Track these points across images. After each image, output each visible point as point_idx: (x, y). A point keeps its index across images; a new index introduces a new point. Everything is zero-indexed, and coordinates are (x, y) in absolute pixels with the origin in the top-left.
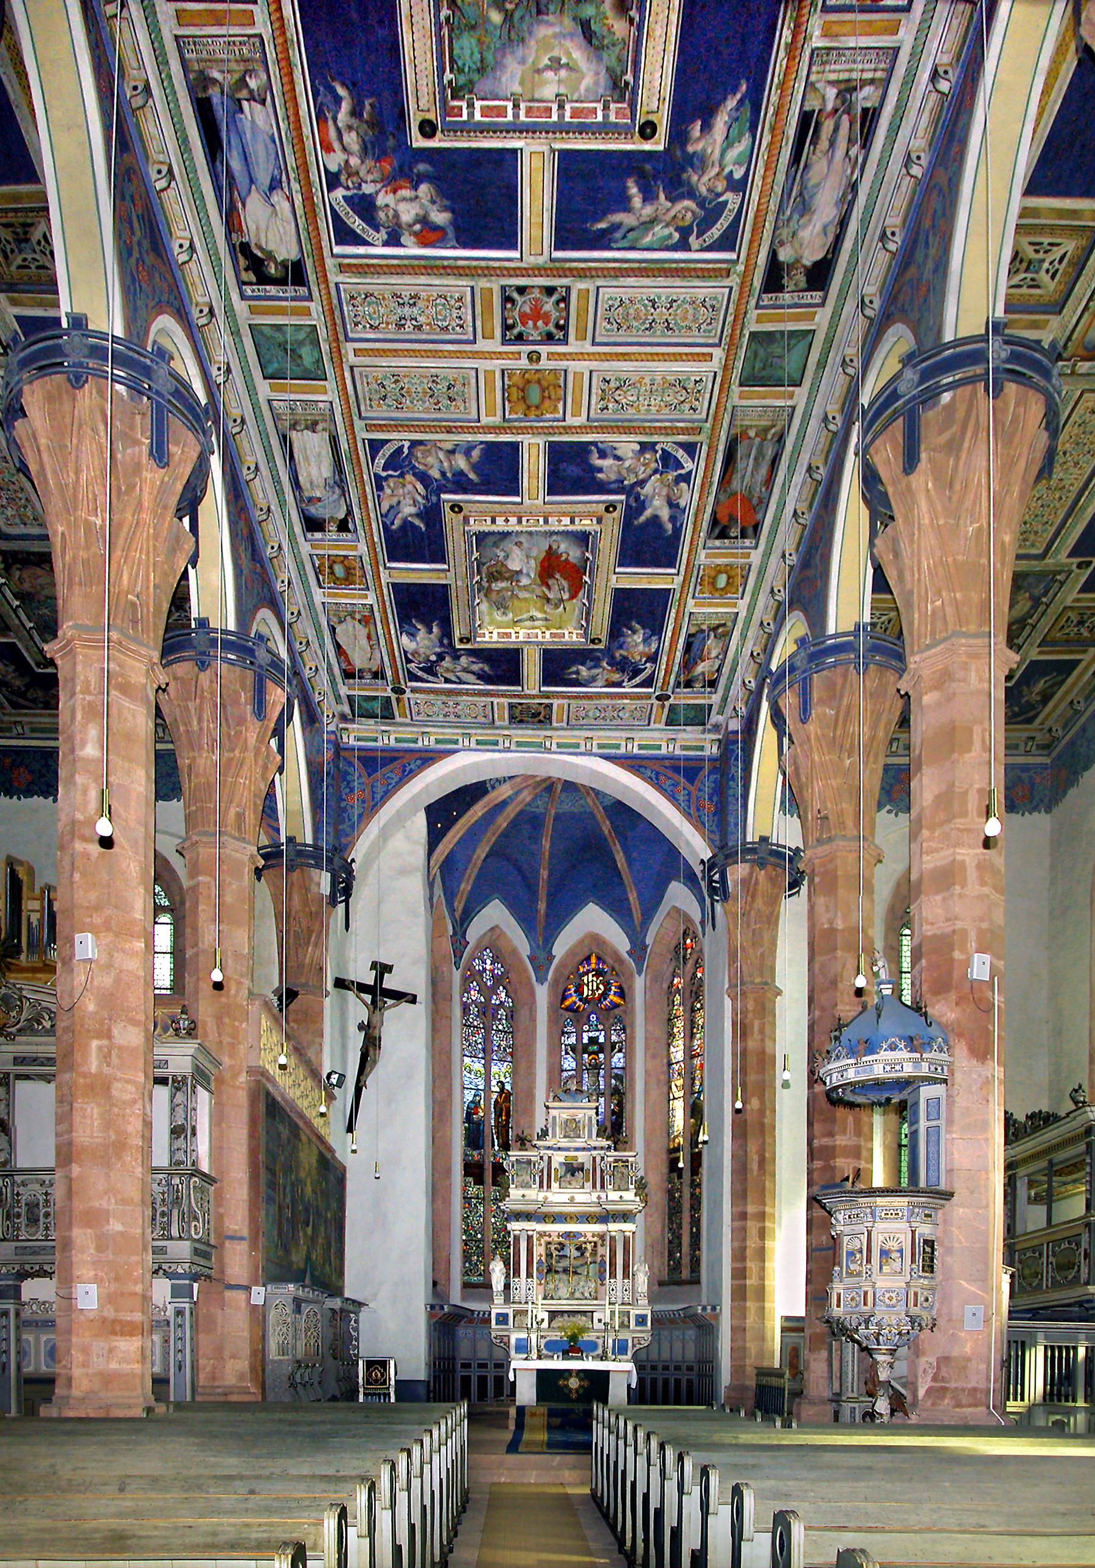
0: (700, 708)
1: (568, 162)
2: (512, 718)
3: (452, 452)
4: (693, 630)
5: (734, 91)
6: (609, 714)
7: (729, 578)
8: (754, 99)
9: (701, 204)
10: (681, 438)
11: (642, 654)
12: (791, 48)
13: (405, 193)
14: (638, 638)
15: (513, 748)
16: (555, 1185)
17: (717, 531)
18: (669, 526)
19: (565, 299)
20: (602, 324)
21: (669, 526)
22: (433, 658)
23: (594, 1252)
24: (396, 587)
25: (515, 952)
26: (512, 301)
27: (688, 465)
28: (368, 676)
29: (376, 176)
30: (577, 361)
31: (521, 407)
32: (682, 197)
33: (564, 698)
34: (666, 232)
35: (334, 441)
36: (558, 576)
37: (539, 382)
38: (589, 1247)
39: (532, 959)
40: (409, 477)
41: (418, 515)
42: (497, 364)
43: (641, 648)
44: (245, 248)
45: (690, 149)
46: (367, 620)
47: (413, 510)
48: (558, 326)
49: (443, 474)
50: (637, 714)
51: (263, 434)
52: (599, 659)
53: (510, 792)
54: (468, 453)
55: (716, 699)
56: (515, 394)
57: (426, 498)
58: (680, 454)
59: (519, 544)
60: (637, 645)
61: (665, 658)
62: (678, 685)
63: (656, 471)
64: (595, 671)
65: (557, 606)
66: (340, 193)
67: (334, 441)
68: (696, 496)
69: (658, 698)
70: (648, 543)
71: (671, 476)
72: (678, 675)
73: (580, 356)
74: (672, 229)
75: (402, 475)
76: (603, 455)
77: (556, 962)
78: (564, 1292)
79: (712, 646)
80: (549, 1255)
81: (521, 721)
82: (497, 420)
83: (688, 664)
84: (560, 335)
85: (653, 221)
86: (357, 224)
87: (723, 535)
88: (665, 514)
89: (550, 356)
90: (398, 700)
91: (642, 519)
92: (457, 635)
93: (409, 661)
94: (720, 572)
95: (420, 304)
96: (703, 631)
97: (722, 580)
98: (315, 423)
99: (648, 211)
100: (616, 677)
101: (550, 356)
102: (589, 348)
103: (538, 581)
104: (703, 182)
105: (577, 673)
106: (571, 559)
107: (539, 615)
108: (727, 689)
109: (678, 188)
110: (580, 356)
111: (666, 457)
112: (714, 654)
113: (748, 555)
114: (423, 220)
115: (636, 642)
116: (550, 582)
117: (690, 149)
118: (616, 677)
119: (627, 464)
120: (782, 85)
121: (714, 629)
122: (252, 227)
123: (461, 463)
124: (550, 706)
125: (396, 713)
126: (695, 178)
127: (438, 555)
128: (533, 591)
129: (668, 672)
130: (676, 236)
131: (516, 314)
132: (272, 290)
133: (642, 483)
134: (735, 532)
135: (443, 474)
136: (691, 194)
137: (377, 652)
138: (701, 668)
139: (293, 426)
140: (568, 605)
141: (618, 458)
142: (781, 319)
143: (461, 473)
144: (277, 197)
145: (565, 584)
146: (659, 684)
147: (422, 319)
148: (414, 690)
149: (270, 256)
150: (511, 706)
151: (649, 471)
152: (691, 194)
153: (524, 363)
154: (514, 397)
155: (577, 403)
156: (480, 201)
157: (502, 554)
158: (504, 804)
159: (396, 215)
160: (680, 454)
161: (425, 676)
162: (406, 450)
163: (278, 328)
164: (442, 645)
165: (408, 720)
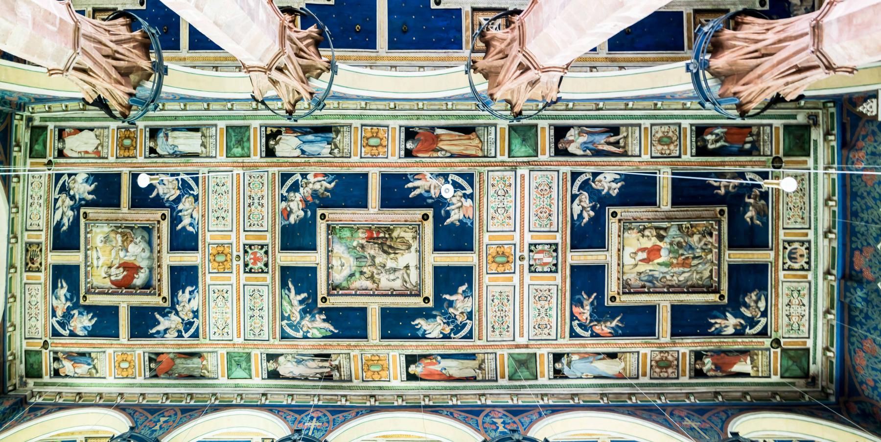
1: (313, 270)
3: (192, 217)
4: (93, 355)
5: (335, 328)
6: (33, 311)
8: (334, 336)
9: (299, 323)
10: (201, 331)
11: (75, 328)
12: (349, 345)
13: (301, 206)
17: (153, 356)
18: (154, 331)
19: (263, 272)
20: (252, 288)
21: (154, 331)
26: (262, 249)
27: (186, 335)
29: (306, 194)
30: (236, 277)
31: (215, 252)
32: (301, 315)
33: (46, 280)
34: (288, 311)
35: (196, 155)
36: (125, 273)
37: (226, 260)
40: (178, 192)
41: (158, 194)
42: (233, 240)
44: (279, 133)
45: (317, 316)
47: (161, 193)
48: (251, 269)
49: (181, 211)
50: (33, 330)
51: (199, 118)
52: (71, 300)
54: (191, 224)
56: (221, 249)
57: (168, 200)
58: (192, 331)
60: (81, 323)
61: (74, 341)
62: (56, 353)
63: (183, 320)
64: (63, 299)
65: (106, 273)
66: (300, 178)
67: (196, 155)
68: (172, 342)
70: (143, 322)
71: (181, 328)
73: (238, 280)
74: (289, 312)
75: (179, 189)
76: (191, 293)
79: (83, 369)
82: (208, 240)
83: (70, 356)
84: (247, 270)
85: (292, 305)
86: (289, 182)
87: (151, 360)
88: (160, 328)
89: (238, 266)
91: (158, 316)
94: (130, 363)
95: (259, 208)
96: (93, 361)
97: (124, 365)
98: (205, 147)
99: (296, 303)
101: (238, 266)
102: (242, 282)
103: (122, 262)
104: (306, 322)
107: (100, 264)
109: (304, 312)
110: (238, 280)
111: (191, 324)
112: (77, 370)
114: (291, 212)
115: (82, 322)
116: (121, 269)
117: (317, 316)
119: (187, 305)
120: (339, 345)
121: (94, 367)
122: (288, 138)
123: (186, 221)
124: (39, 271)
126: (307, 319)
128: (115, 259)
129: (63, 345)
130: (286, 315)
131: (256, 250)
132: (264, 140)
133: (177, 313)
134: (153, 365)
135: (181, 211)
136: (302, 318)
139: (203, 135)
140: (108, 280)
141: (190, 300)
142: (256, 363)
143: (181, 221)
144: (298, 152)
145: (120, 277)
146: (55, 341)
147: (253, 207)
149: (277, 143)
151: (183, 317)
152: (302, 318)
153: (235, 254)
154: (219, 249)
155: (216, 279)
156: (297, 236)
159: (292, 201)
160: (192, 331)
162: (192, 192)
163: (249, 140)
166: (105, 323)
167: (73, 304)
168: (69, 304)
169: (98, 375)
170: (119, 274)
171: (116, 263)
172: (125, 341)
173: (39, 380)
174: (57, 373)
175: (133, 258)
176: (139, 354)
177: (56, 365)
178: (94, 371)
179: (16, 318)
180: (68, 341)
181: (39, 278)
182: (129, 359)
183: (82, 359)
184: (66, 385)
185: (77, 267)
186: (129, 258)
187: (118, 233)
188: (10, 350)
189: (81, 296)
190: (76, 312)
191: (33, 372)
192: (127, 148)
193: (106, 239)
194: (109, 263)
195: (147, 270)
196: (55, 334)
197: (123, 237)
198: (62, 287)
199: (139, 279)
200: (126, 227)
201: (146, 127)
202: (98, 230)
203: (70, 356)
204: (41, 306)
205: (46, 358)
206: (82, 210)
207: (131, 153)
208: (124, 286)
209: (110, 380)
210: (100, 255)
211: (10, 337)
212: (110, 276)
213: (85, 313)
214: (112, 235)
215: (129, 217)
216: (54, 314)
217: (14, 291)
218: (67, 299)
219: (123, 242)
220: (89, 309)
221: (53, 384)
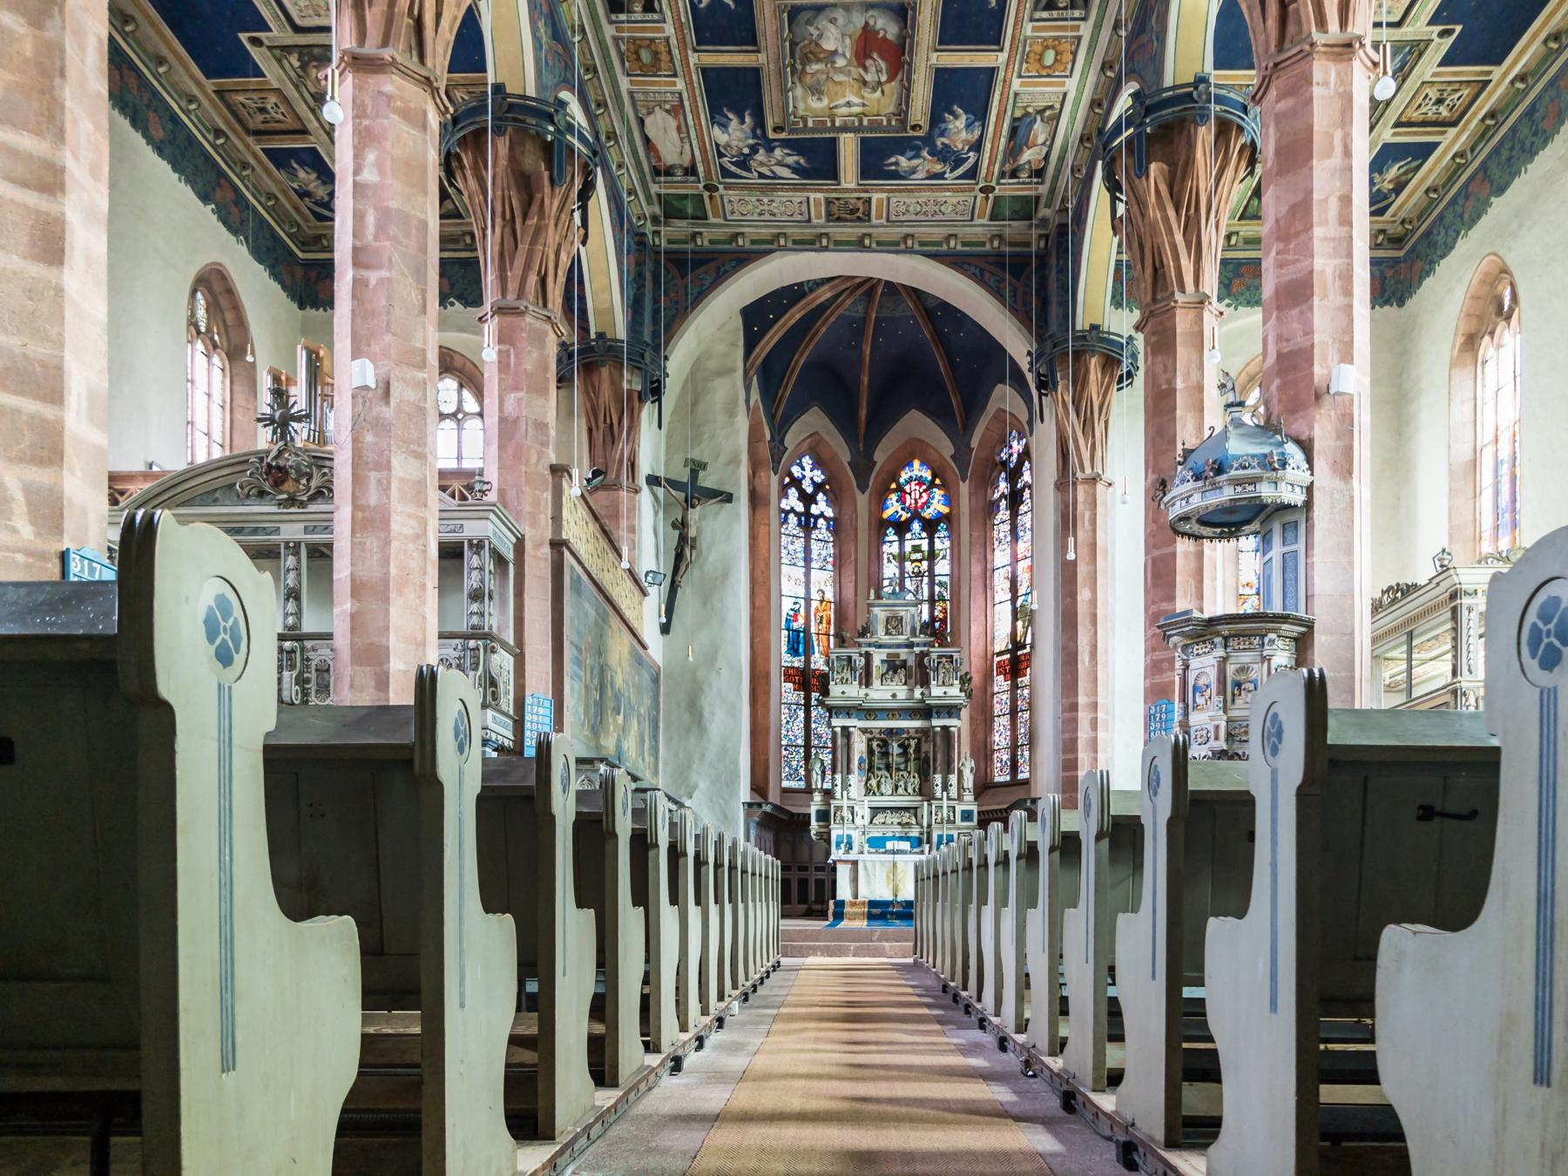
0: (1026, 199)
2: (829, 214)
4: (1018, 114)
6: (931, 208)
7: (1057, 54)
11: (965, 142)
14: (961, 123)
15: (831, 246)
22: (746, 151)
24: (705, 71)
28: (679, 172)
33: (883, 191)
36: (875, 56)
43: (964, 135)
46: (677, 110)
50: (960, 208)
53: (829, 295)
55: (1043, 190)
59: (833, 21)
60: (959, 131)
62: (1002, 175)
64: (916, 162)
65: (874, 90)
69: (981, 190)
72: (1003, 164)
79: (1040, 131)
80: (871, 752)
81: (839, 219)
83: (1013, 151)
90: (711, 197)
92: (770, 124)
93: (721, 155)
94: (1047, 48)
96: (1027, 114)
97: (1049, 57)
100: (938, 168)
105: (896, 164)
106: (889, 36)
107: (856, 100)
108: (1056, 178)
112: (1041, 140)
113: (1077, 28)
115: (958, 129)
116: (869, 62)
118: (938, 168)
121: (1041, 112)
124: (869, 201)
125: (710, 213)
127: (749, 38)
128: (849, 74)
129: (992, 163)
137: (687, 147)
138: (1027, 155)
140: (887, 88)
145: (883, 65)
148: (728, 187)
150: (828, 202)
157: (815, 33)
158: (821, 309)
161: (739, 171)
164: (755, 136)
165: (720, 221)
166: (964, 92)
167: (926, 145)
168: (925, 153)
169: (1058, 106)
170: (877, 68)
171: (857, 71)
172: (1002, 57)
173: (1043, 201)
174: (1039, 173)
175: (848, 41)
176: (1034, 29)
177: (1024, 175)
178: (1048, 113)
179: (938, 233)
180: (987, 155)
181: (880, 201)
182: (1038, 48)
183: (1021, 132)
184: (1062, 158)
185: (864, 142)
186: (847, 48)
187: (803, 70)
188: (984, 244)
189: (911, 133)
190: (939, 142)
191: (1025, 209)
192: (656, 55)
193: (817, 91)
194: (856, 85)
195: (871, 13)
196: (972, 173)
197: (810, 61)
198: (896, 164)
199: (887, 28)
200: (792, 56)
201: (611, 22)
202: (801, 106)
203: (1013, 151)
204: (925, 196)
205: (1008, 189)
206: (771, 135)
207: (662, 49)
208: (898, 57)
209: (1071, 85)
210: (842, 101)
211: (964, 244)
212: (879, 83)
213: (943, 126)
214: (808, 79)
215: (772, 50)
216: (941, 176)
217: (896, 238)
218: (917, 156)
219: (819, 60)
220: (936, 118)
221: (1056, 178)
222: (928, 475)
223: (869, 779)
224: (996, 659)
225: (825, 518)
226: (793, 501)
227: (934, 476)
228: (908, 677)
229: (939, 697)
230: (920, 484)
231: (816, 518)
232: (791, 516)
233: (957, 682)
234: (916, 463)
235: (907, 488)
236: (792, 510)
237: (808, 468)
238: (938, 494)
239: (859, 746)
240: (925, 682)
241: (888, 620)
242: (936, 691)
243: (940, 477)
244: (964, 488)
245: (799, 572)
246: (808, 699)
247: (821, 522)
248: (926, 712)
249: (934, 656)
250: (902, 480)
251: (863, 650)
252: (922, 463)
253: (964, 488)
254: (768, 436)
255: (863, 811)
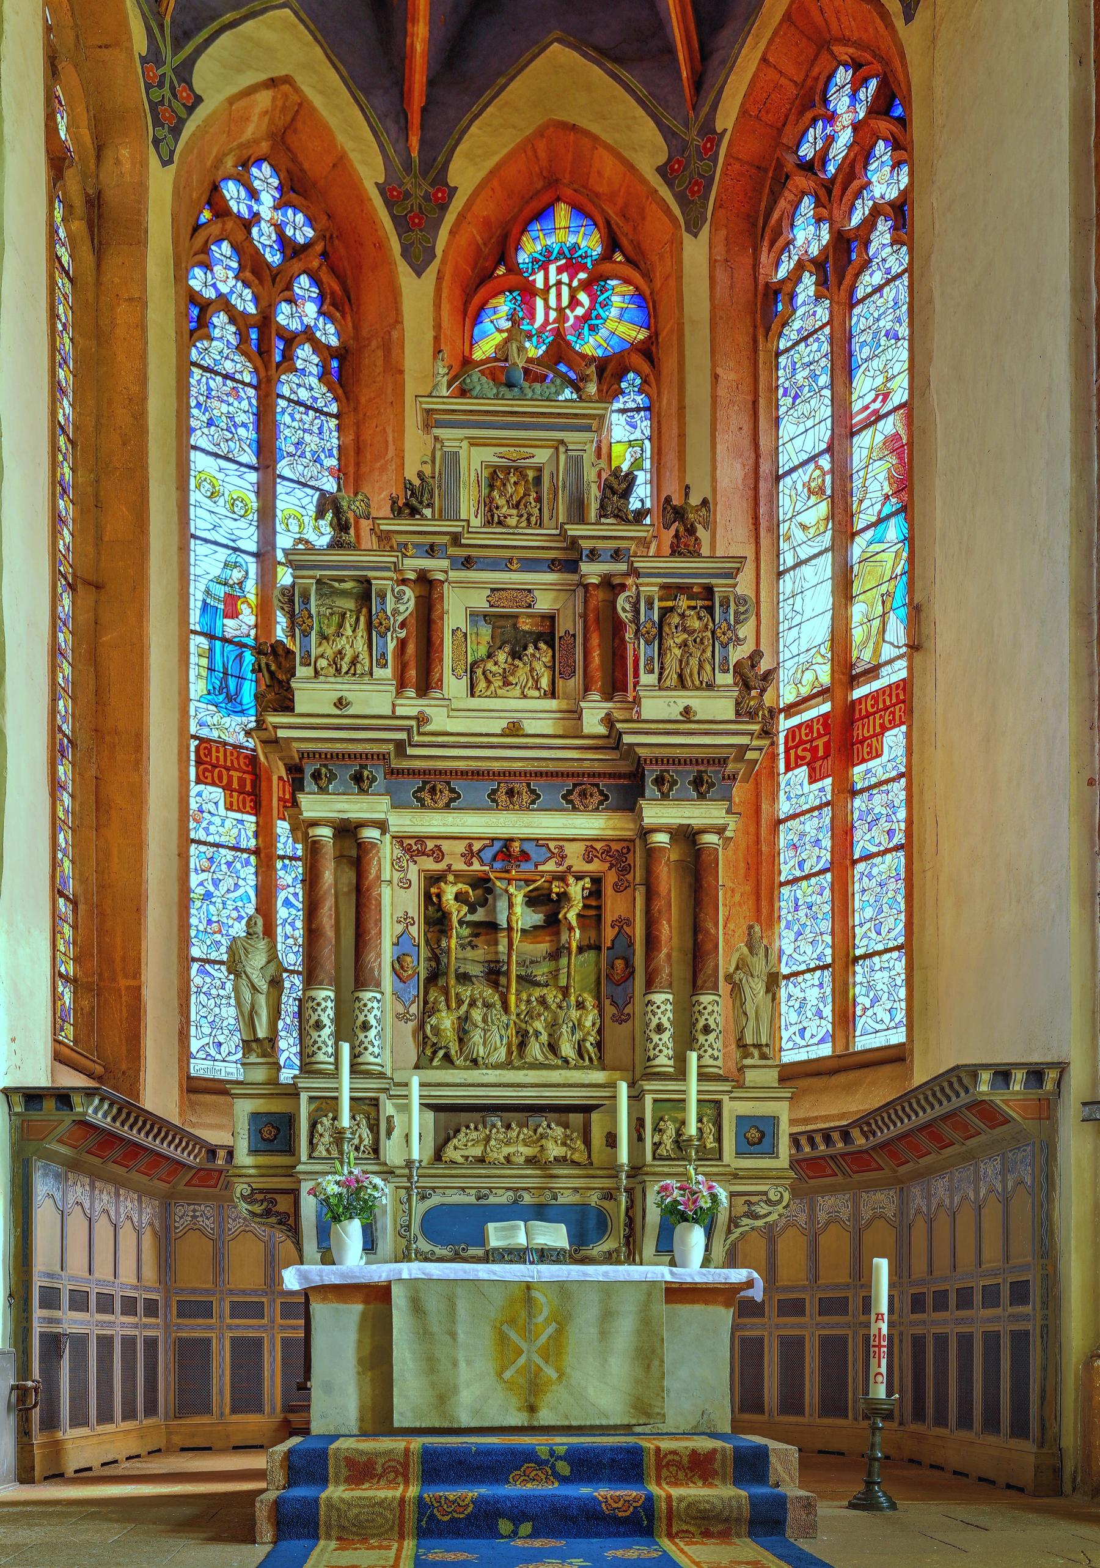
16: (454, 686)
23: (593, 915)
25: (341, 162)
38: (576, 890)
39: (391, 195)
77: (457, 205)
78: (492, 1039)
80: (437, 921)
222: (591, 244)
223: (428, 1010)
224: (785, 724)
225: (318, 347)
226: (220, 278)
227: (612, 244)
228: (560, 670)
229: (666, 725)
230: (572, 266)
231: (291, 340)
232: (220, 319)
233: (727, 679)
234: (562, 212)
235: (539, 280)
236: (224, 303)
237: (267, 199)
238: (618, 297)
239: (397, 904)
240: (616, 683)
241: (495, 478)
242: (657, 706)
243: (627, 250)
244: (696, 252)
245: (242, 484)
246: (265, 832)
247: (304, 353)
248: (625, 780)
249: (650, 588)
250: (523, 258)
251: (413, 564)
252: (579, 210)
253: (696, 252)
254: (140, 44)
255: (412, 1134)
